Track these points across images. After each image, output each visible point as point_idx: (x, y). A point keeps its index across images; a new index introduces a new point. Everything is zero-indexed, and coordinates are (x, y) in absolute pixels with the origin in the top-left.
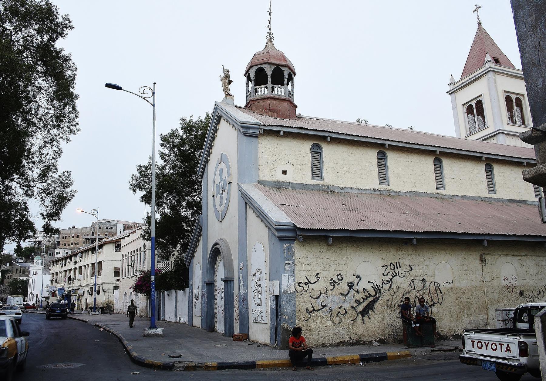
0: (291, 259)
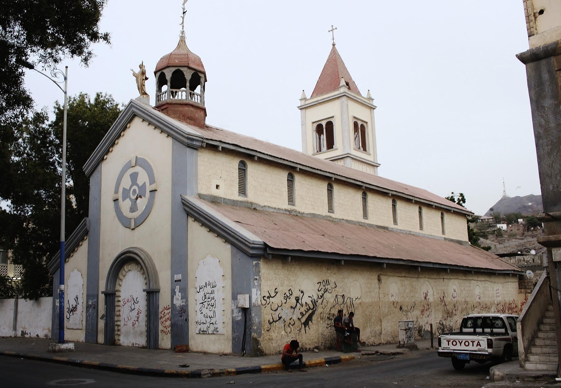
0: (258, 275)
